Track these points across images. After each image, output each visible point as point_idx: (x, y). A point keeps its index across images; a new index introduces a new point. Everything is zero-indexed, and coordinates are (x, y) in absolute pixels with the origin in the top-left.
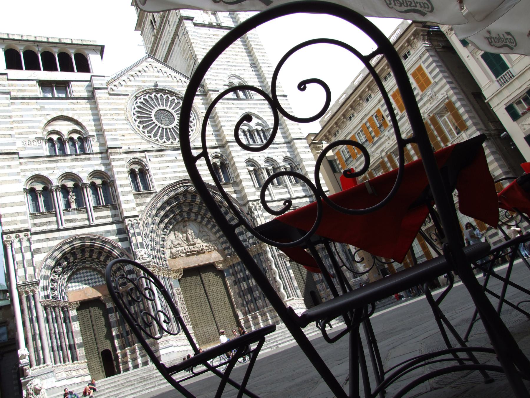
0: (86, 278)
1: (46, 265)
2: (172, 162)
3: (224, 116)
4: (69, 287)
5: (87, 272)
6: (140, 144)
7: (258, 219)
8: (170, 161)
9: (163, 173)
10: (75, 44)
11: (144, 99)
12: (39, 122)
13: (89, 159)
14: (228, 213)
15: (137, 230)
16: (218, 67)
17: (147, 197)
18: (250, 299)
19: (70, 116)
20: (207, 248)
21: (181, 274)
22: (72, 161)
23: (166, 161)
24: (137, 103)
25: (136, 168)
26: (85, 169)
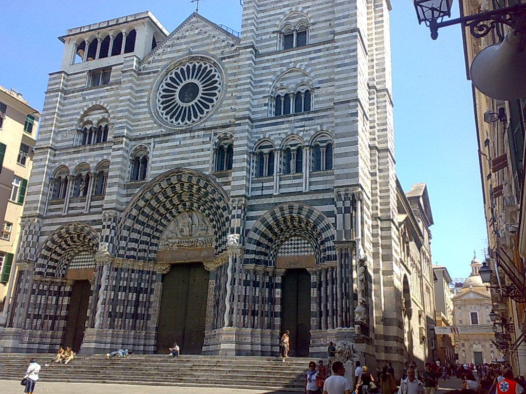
0: (84, 260)
1: (46, 245)
3: (244, 84)
4: (70, 266)
5: (86, 255)
7: (232, 220)
9: (161, 161)
10: (129, 22)
11: (176, 73)
12: (78, 113)
13: (102, 149)
15: (109, 223)
19: (101, 104)
22: (89, 152)
23: (169, 147)
24: (166, 80)
25: (141, 154)
26: (96, 159)
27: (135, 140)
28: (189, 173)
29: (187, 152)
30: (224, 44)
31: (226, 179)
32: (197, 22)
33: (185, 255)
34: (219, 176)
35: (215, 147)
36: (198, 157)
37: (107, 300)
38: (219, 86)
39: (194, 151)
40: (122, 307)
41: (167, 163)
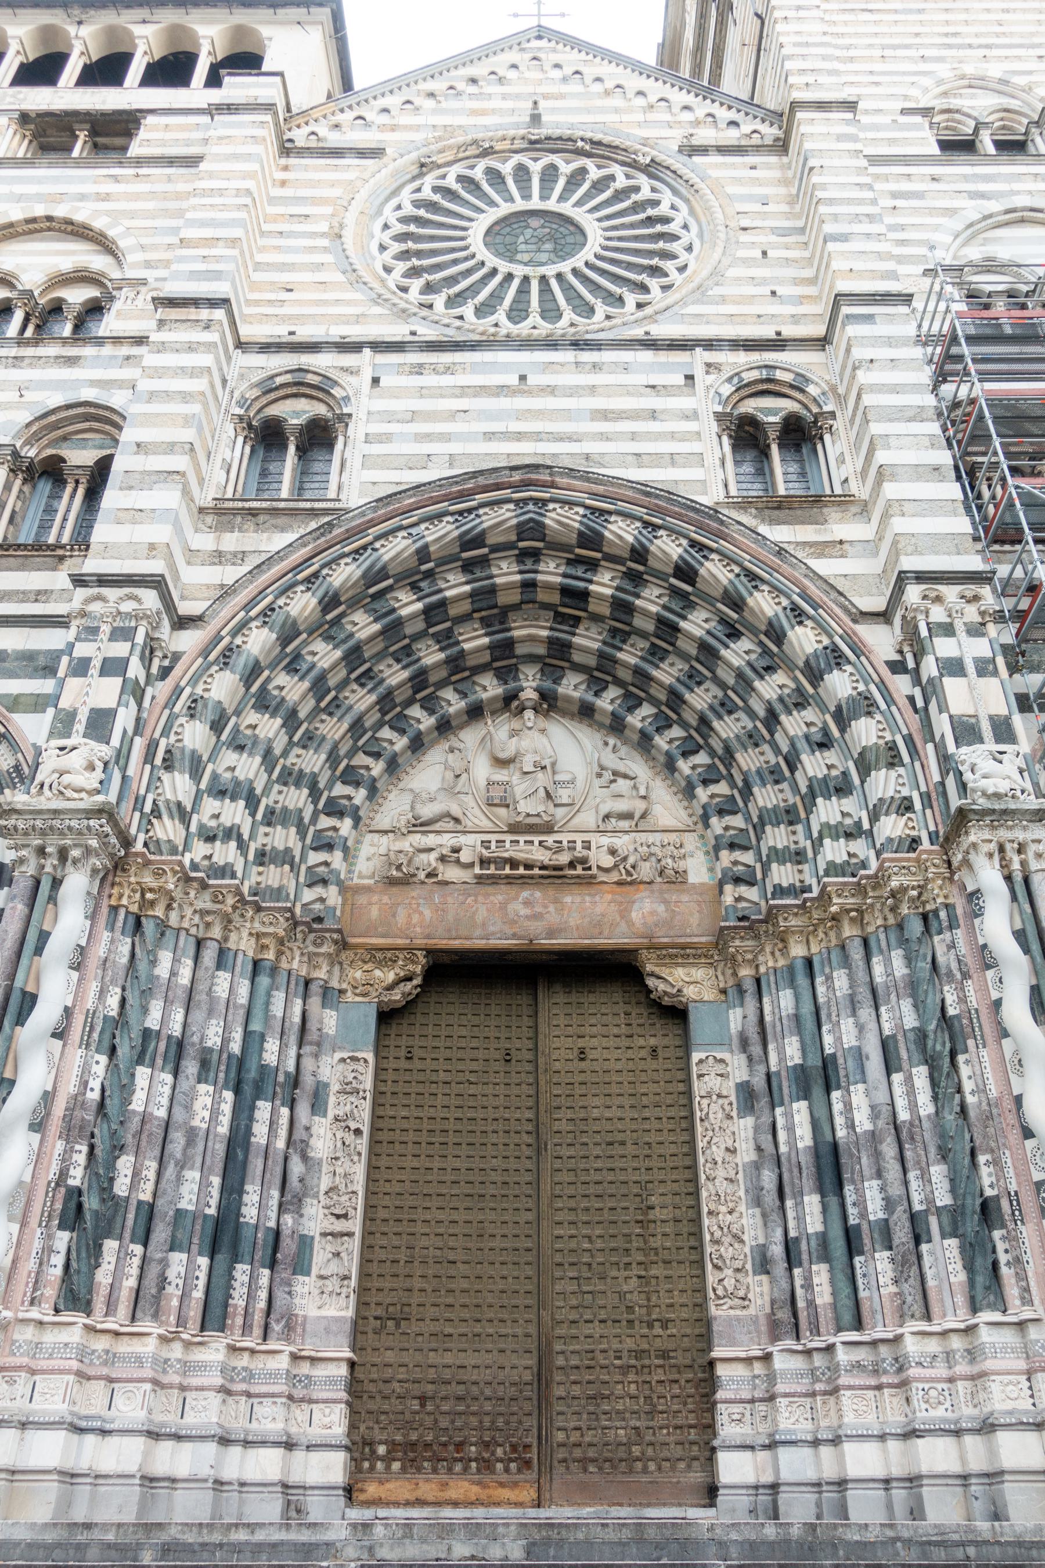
2: (498, 395)
6: (358, 319)
8: (482, 390)
14: (770, 669)
16: (887, 53)
17: (283, 530)
18: (814, 1224)
20: (608, 861)
21: (409, 979)
23: (463, 391)
27: (267, 348)
28: (594, 495)
29: (567, 414)
30: (687, 116)
31: (818, 532)
32: (554, 50)
33: (524, 911)
34: (773, 522)
35: (719, 409)
36: (634, 436)
37: (59, 1109)
38: (682, 233)
39: (604, 415)
40: (151, 1168)
41: (455, 448)
